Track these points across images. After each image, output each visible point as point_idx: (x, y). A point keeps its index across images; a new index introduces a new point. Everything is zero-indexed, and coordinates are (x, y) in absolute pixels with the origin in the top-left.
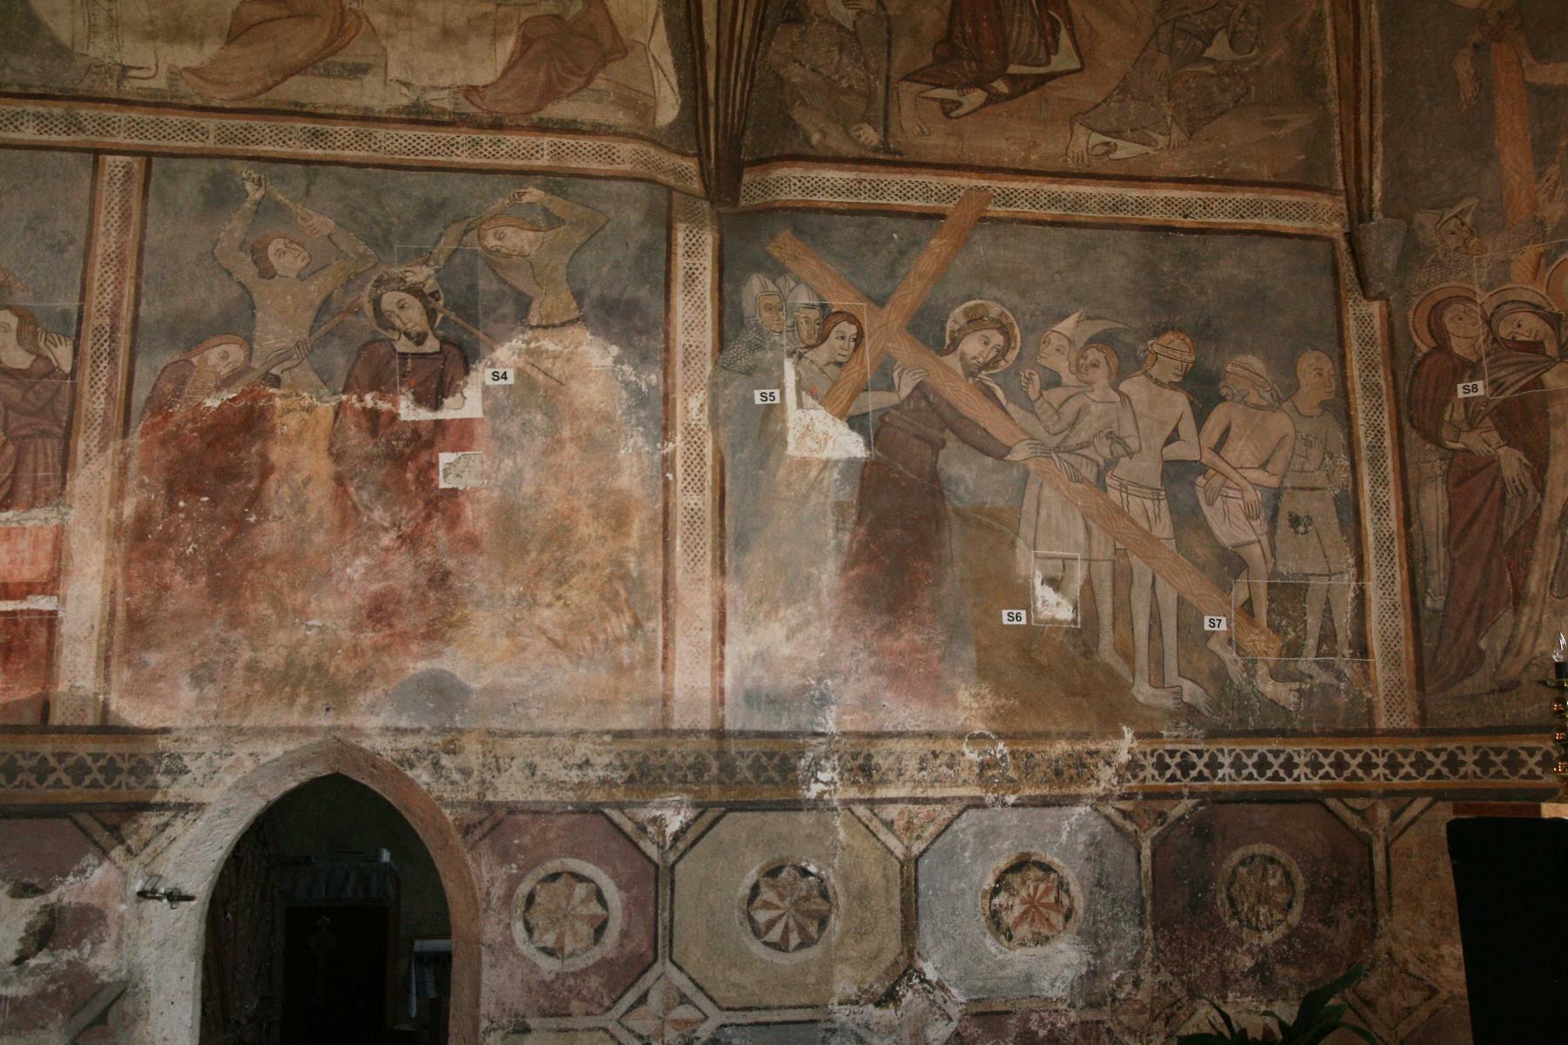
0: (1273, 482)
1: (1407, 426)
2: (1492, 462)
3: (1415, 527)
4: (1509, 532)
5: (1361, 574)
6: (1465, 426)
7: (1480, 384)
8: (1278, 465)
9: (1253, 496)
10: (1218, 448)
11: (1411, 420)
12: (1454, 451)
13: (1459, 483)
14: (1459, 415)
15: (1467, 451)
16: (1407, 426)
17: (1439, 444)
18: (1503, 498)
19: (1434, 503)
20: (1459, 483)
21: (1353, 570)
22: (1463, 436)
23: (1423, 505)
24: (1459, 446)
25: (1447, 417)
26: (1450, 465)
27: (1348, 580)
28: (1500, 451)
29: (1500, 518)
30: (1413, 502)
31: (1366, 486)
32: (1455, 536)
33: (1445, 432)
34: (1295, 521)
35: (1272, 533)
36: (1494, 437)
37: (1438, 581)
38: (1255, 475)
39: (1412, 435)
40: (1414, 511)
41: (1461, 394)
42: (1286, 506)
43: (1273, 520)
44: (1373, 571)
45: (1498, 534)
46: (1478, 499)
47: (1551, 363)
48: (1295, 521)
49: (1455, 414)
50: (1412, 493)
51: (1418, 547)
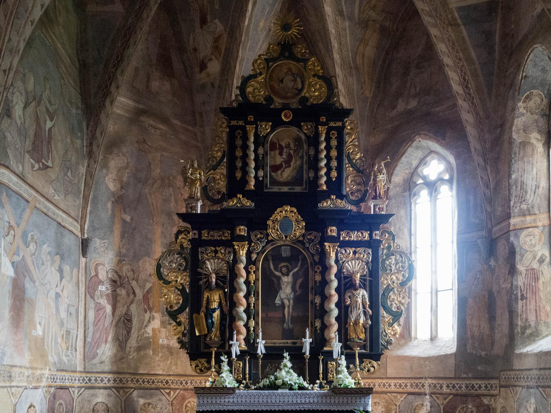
0: (68, 302)
1: (87, 293)
2: (104, 307)
3: (87, 320)
4: (106, 325)
5: (77, 331)
6: (100, 297)
7: (104, 287)
8: (69, 298)
9: (66, 306)
10: (62, 291)
11: (88, 292)
12: (97, 303)
13: (97, 311)
14: (99, 294)
15: (100, 303)
16: (87, 293)
17: (94, 300)
18: (105, 317)
19: (91, 315)
20: (97, 311)
21: (77, 329)
22: (99, 299)
23: (89, 314)
24: (98, 301)
25: (96, 293)
26: (96, 306)
27: (75, 331)
28: (107, 305)
29: (105, 321)
30: (87, 313)
31: (80, 307)
32: (95, 324)
33: (96, 298)
34: (70, 314)
35: (67, 317)
36: (106, 301)
37: (90, 335)
38: (66, 299)
39: (88, 296)
40: (87, 316)
41: (100, 289)
42: (69, 310)
43: (68, 313)
44: (79, 330)
45: (104, 325)
46: (101, 316)
47: (118, 287)
48: (70, 314)
49: (98, 293)
50: (87, 311)
51: (87, 325)
